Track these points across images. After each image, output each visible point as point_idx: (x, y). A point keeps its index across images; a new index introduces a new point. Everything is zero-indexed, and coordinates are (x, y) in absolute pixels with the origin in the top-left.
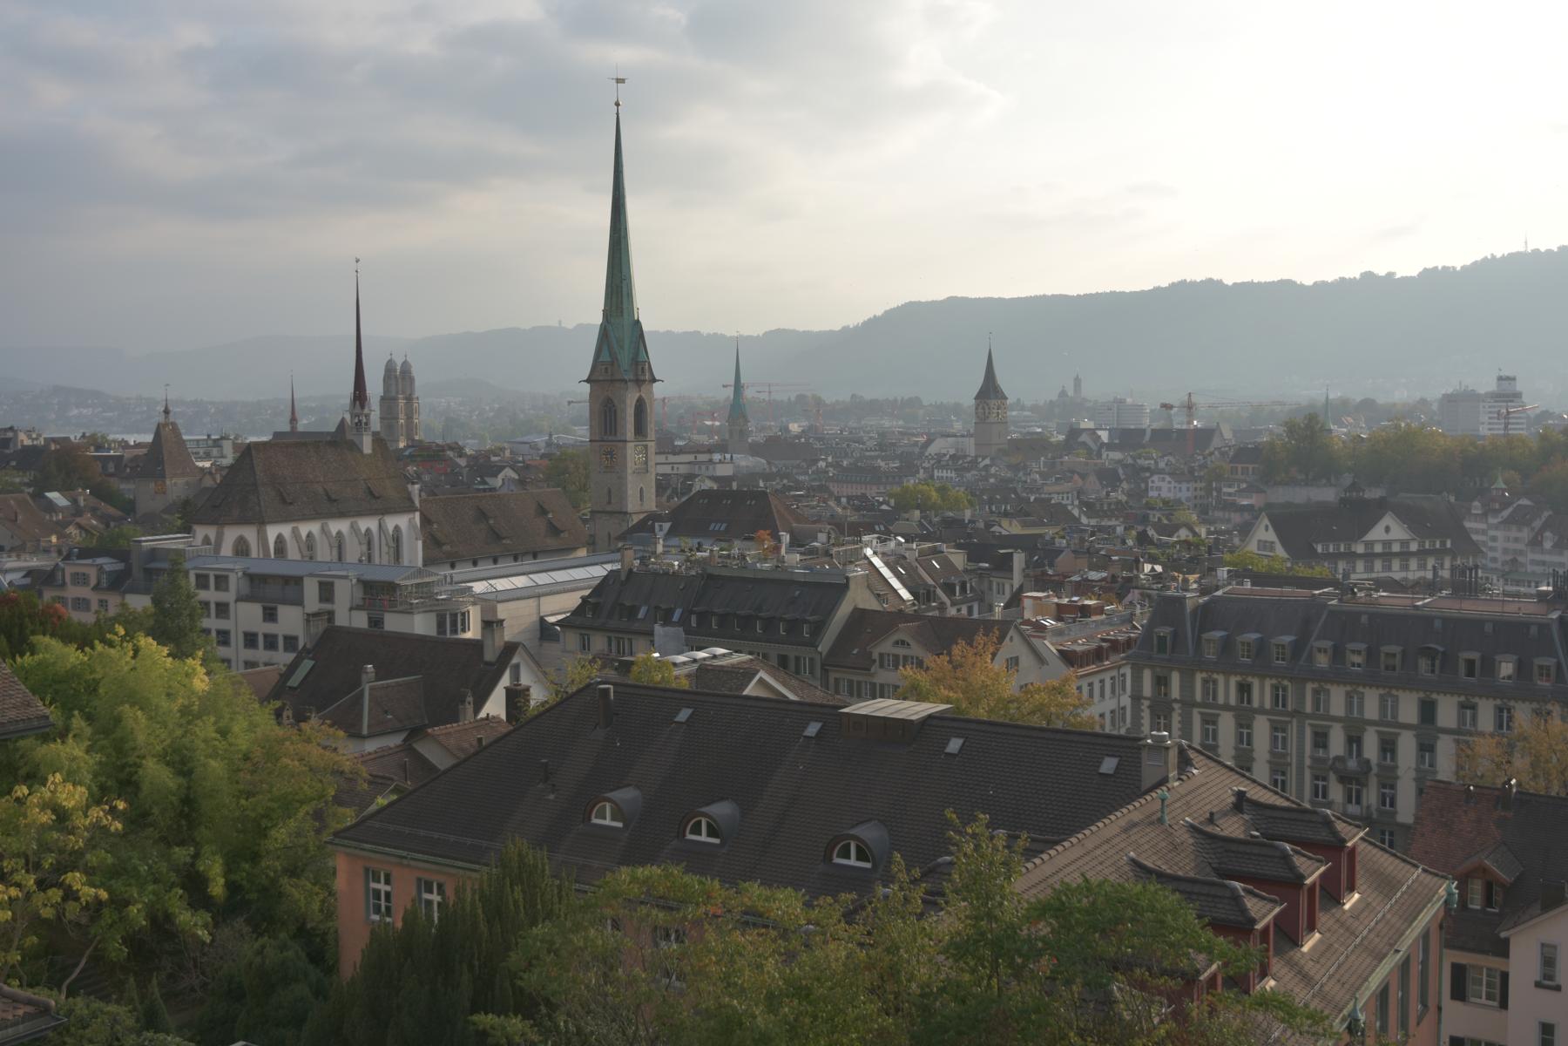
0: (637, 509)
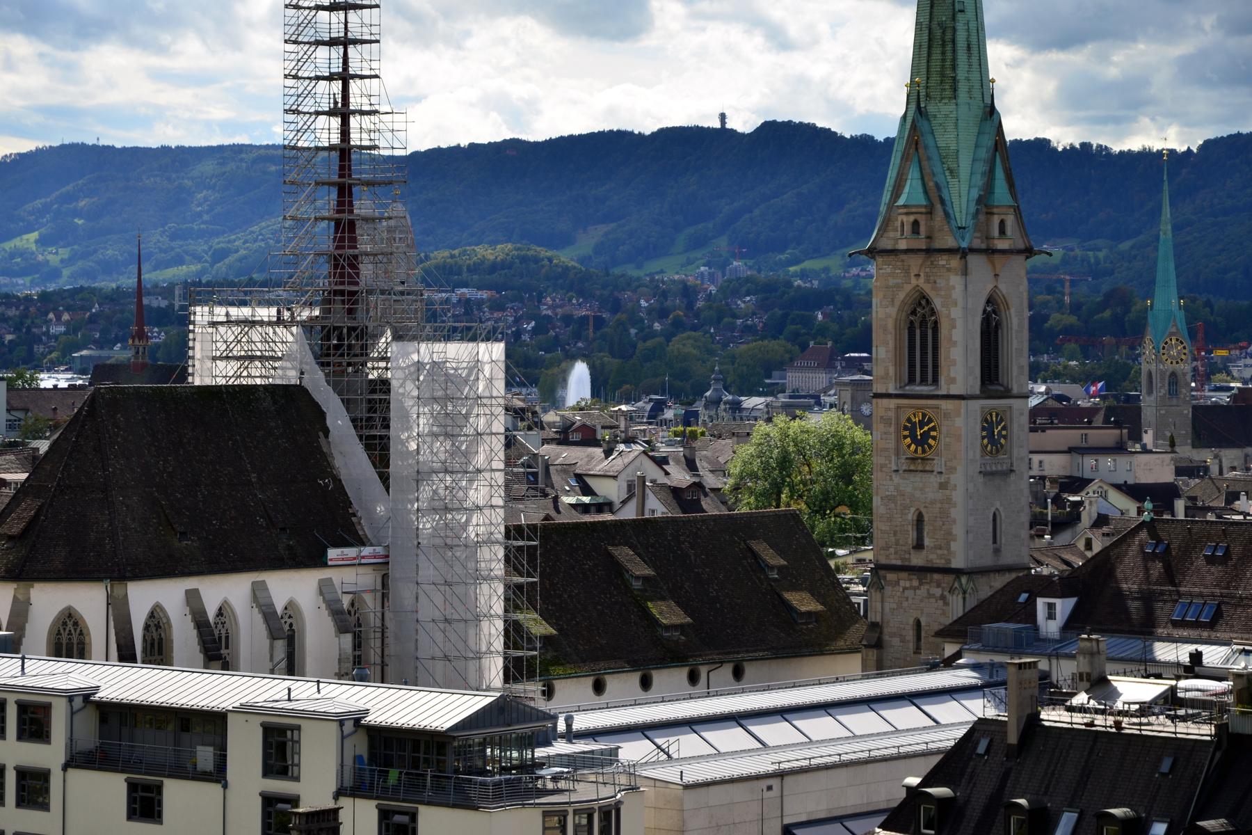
0: (988, 561)
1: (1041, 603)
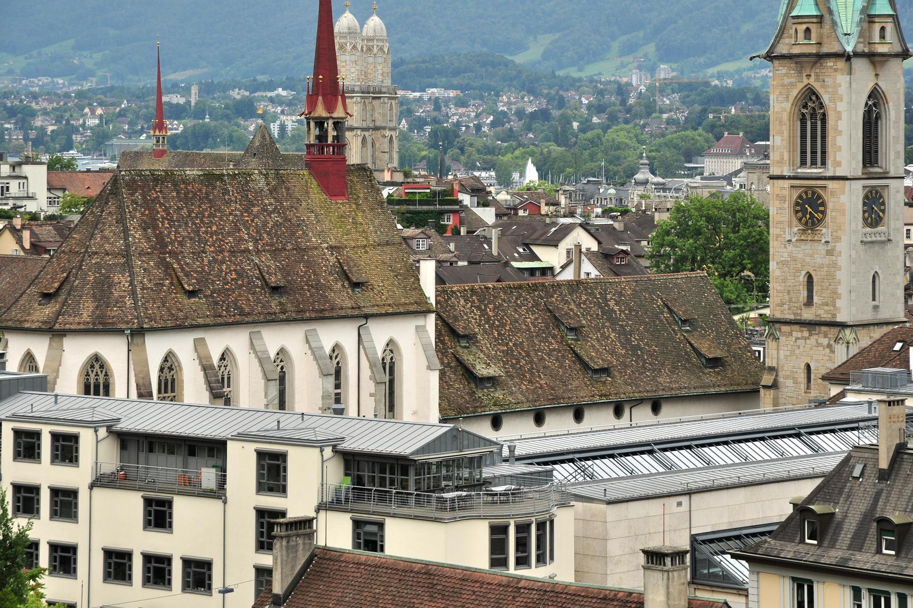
0: (867, 316)
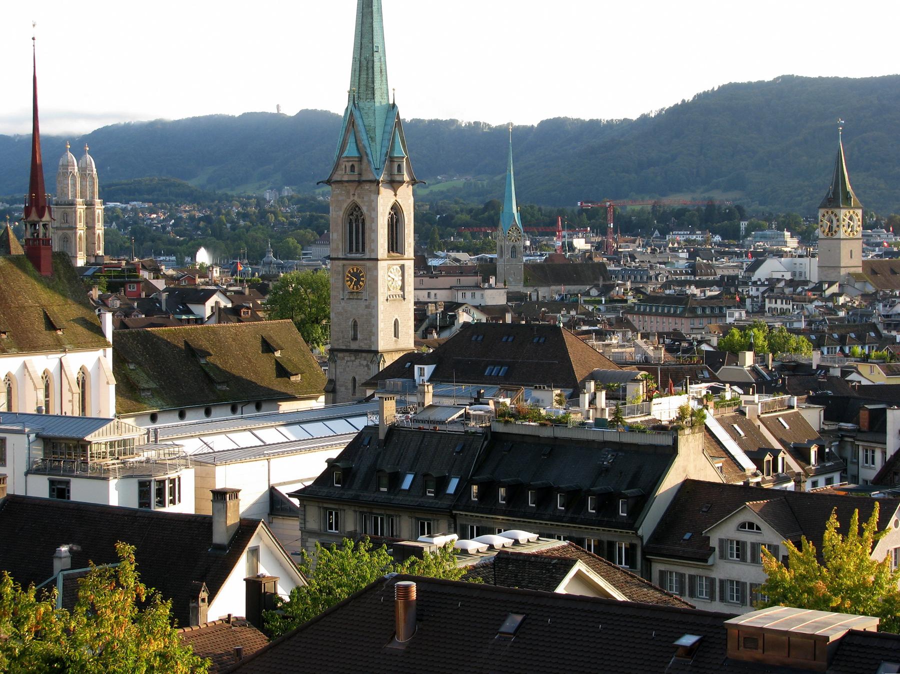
1: (416, 367)
